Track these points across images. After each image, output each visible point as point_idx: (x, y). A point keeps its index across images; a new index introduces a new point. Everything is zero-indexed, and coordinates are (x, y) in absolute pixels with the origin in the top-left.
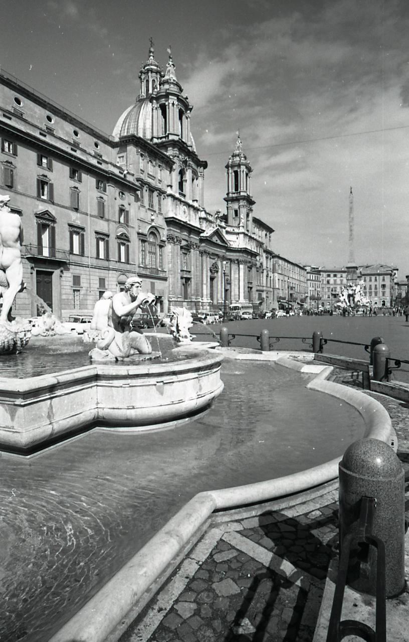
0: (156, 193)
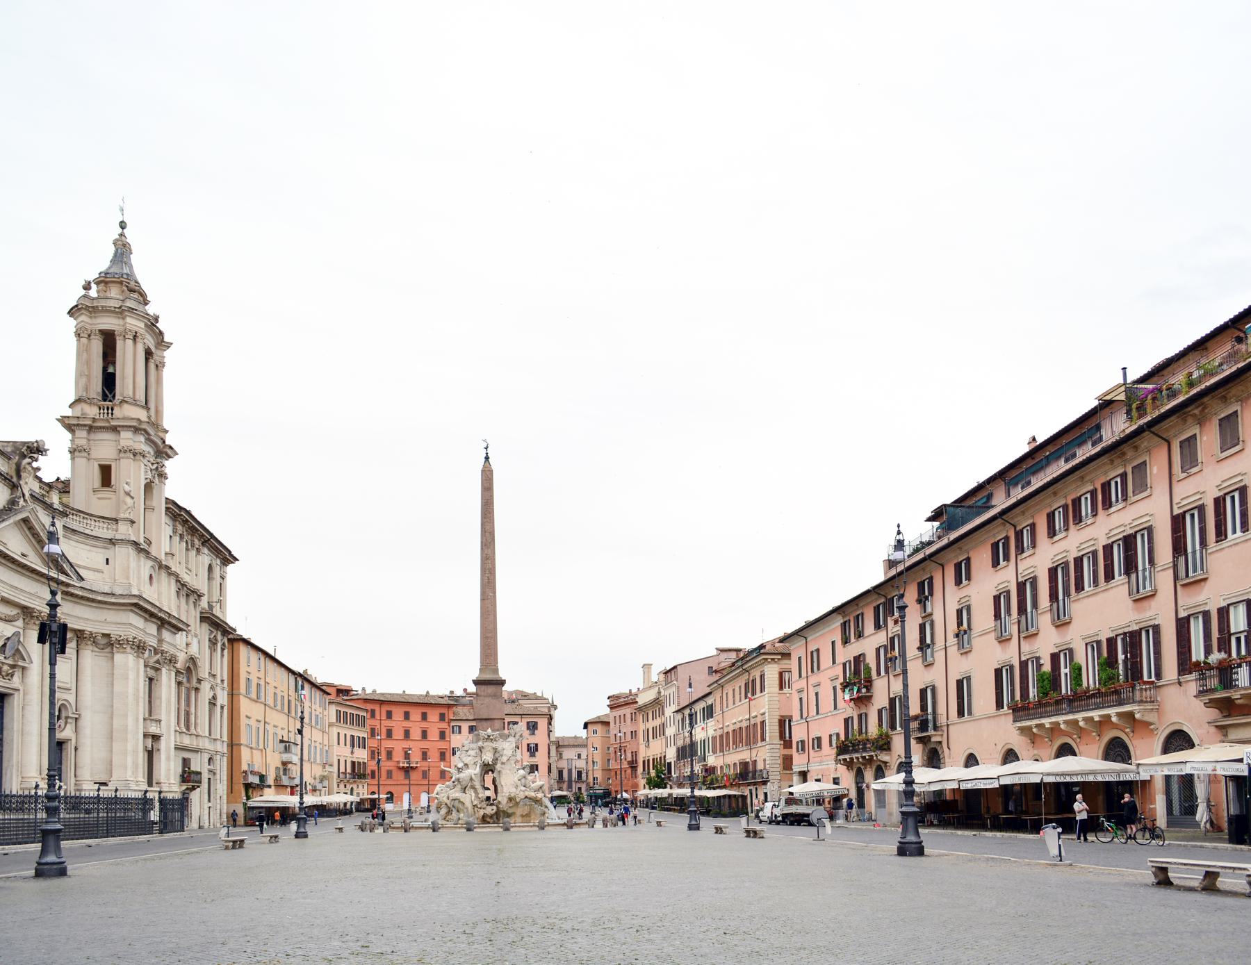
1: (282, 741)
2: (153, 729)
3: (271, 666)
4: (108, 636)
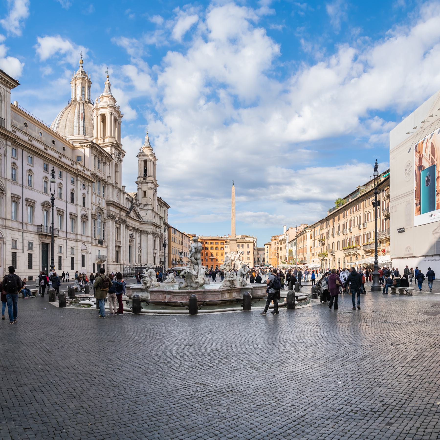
0: (101, 183)
2: (155, 252)
3: (177, 232)
4: (147, 231)
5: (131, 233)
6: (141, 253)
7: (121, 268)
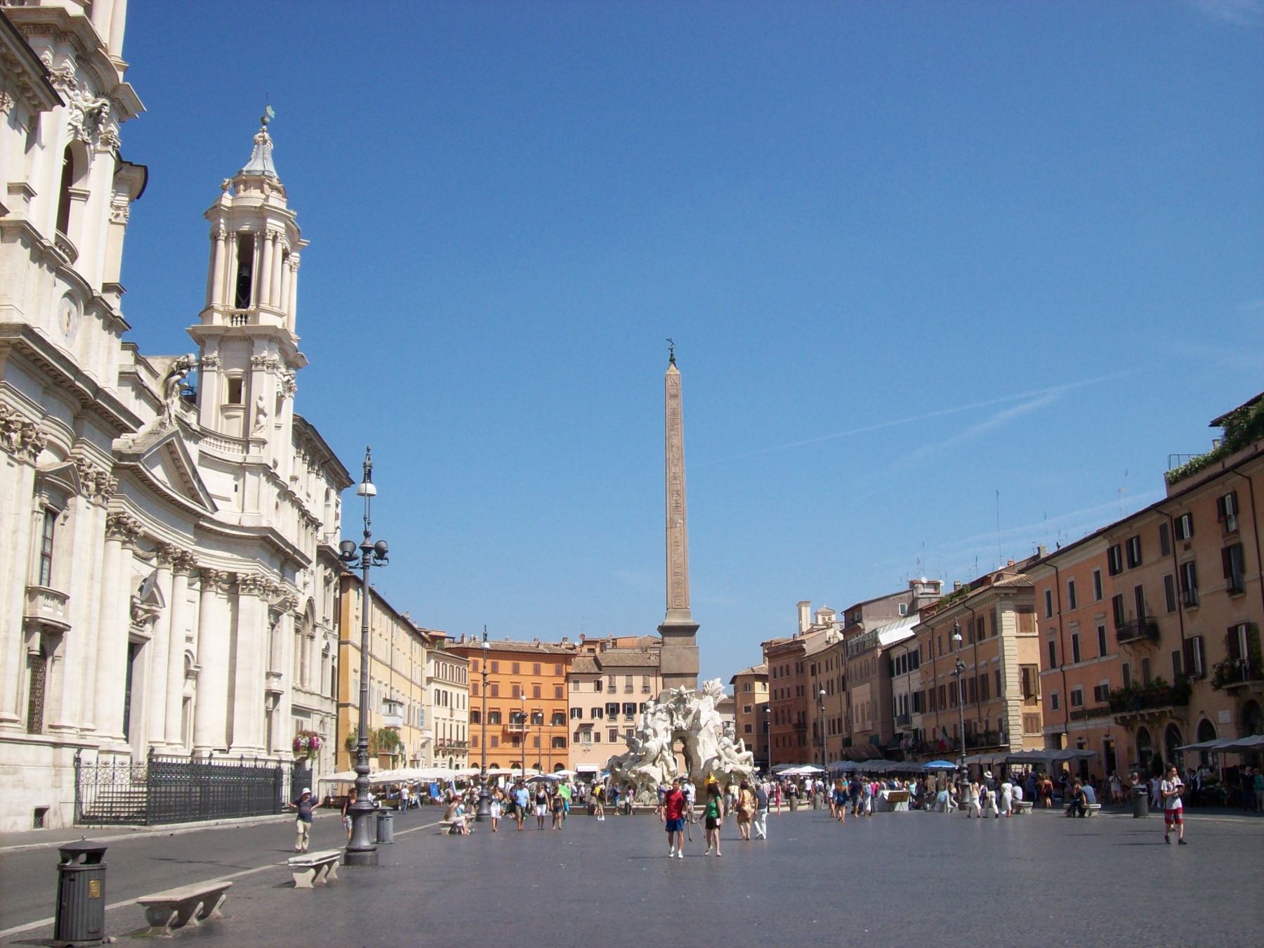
1: (385, 701)
2: (275, 685)
4: (233, 577)
5: (146, 571)
6: (197, 688)
7: (57, 767)
